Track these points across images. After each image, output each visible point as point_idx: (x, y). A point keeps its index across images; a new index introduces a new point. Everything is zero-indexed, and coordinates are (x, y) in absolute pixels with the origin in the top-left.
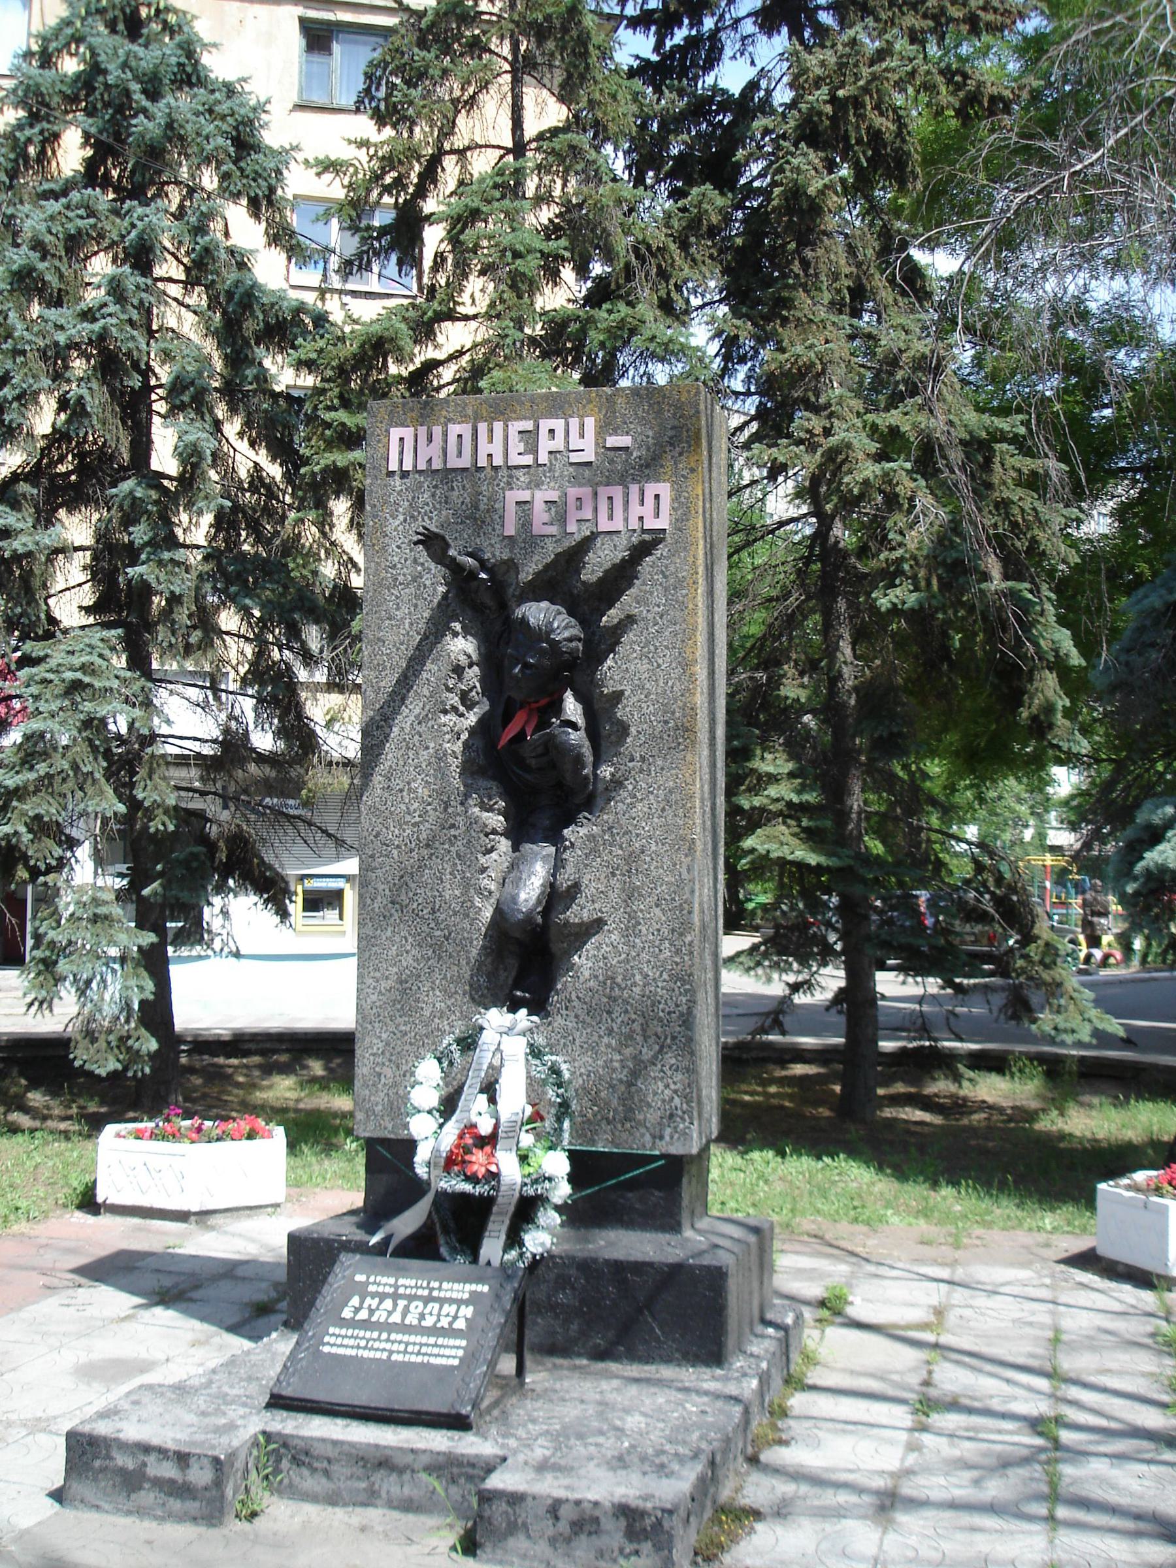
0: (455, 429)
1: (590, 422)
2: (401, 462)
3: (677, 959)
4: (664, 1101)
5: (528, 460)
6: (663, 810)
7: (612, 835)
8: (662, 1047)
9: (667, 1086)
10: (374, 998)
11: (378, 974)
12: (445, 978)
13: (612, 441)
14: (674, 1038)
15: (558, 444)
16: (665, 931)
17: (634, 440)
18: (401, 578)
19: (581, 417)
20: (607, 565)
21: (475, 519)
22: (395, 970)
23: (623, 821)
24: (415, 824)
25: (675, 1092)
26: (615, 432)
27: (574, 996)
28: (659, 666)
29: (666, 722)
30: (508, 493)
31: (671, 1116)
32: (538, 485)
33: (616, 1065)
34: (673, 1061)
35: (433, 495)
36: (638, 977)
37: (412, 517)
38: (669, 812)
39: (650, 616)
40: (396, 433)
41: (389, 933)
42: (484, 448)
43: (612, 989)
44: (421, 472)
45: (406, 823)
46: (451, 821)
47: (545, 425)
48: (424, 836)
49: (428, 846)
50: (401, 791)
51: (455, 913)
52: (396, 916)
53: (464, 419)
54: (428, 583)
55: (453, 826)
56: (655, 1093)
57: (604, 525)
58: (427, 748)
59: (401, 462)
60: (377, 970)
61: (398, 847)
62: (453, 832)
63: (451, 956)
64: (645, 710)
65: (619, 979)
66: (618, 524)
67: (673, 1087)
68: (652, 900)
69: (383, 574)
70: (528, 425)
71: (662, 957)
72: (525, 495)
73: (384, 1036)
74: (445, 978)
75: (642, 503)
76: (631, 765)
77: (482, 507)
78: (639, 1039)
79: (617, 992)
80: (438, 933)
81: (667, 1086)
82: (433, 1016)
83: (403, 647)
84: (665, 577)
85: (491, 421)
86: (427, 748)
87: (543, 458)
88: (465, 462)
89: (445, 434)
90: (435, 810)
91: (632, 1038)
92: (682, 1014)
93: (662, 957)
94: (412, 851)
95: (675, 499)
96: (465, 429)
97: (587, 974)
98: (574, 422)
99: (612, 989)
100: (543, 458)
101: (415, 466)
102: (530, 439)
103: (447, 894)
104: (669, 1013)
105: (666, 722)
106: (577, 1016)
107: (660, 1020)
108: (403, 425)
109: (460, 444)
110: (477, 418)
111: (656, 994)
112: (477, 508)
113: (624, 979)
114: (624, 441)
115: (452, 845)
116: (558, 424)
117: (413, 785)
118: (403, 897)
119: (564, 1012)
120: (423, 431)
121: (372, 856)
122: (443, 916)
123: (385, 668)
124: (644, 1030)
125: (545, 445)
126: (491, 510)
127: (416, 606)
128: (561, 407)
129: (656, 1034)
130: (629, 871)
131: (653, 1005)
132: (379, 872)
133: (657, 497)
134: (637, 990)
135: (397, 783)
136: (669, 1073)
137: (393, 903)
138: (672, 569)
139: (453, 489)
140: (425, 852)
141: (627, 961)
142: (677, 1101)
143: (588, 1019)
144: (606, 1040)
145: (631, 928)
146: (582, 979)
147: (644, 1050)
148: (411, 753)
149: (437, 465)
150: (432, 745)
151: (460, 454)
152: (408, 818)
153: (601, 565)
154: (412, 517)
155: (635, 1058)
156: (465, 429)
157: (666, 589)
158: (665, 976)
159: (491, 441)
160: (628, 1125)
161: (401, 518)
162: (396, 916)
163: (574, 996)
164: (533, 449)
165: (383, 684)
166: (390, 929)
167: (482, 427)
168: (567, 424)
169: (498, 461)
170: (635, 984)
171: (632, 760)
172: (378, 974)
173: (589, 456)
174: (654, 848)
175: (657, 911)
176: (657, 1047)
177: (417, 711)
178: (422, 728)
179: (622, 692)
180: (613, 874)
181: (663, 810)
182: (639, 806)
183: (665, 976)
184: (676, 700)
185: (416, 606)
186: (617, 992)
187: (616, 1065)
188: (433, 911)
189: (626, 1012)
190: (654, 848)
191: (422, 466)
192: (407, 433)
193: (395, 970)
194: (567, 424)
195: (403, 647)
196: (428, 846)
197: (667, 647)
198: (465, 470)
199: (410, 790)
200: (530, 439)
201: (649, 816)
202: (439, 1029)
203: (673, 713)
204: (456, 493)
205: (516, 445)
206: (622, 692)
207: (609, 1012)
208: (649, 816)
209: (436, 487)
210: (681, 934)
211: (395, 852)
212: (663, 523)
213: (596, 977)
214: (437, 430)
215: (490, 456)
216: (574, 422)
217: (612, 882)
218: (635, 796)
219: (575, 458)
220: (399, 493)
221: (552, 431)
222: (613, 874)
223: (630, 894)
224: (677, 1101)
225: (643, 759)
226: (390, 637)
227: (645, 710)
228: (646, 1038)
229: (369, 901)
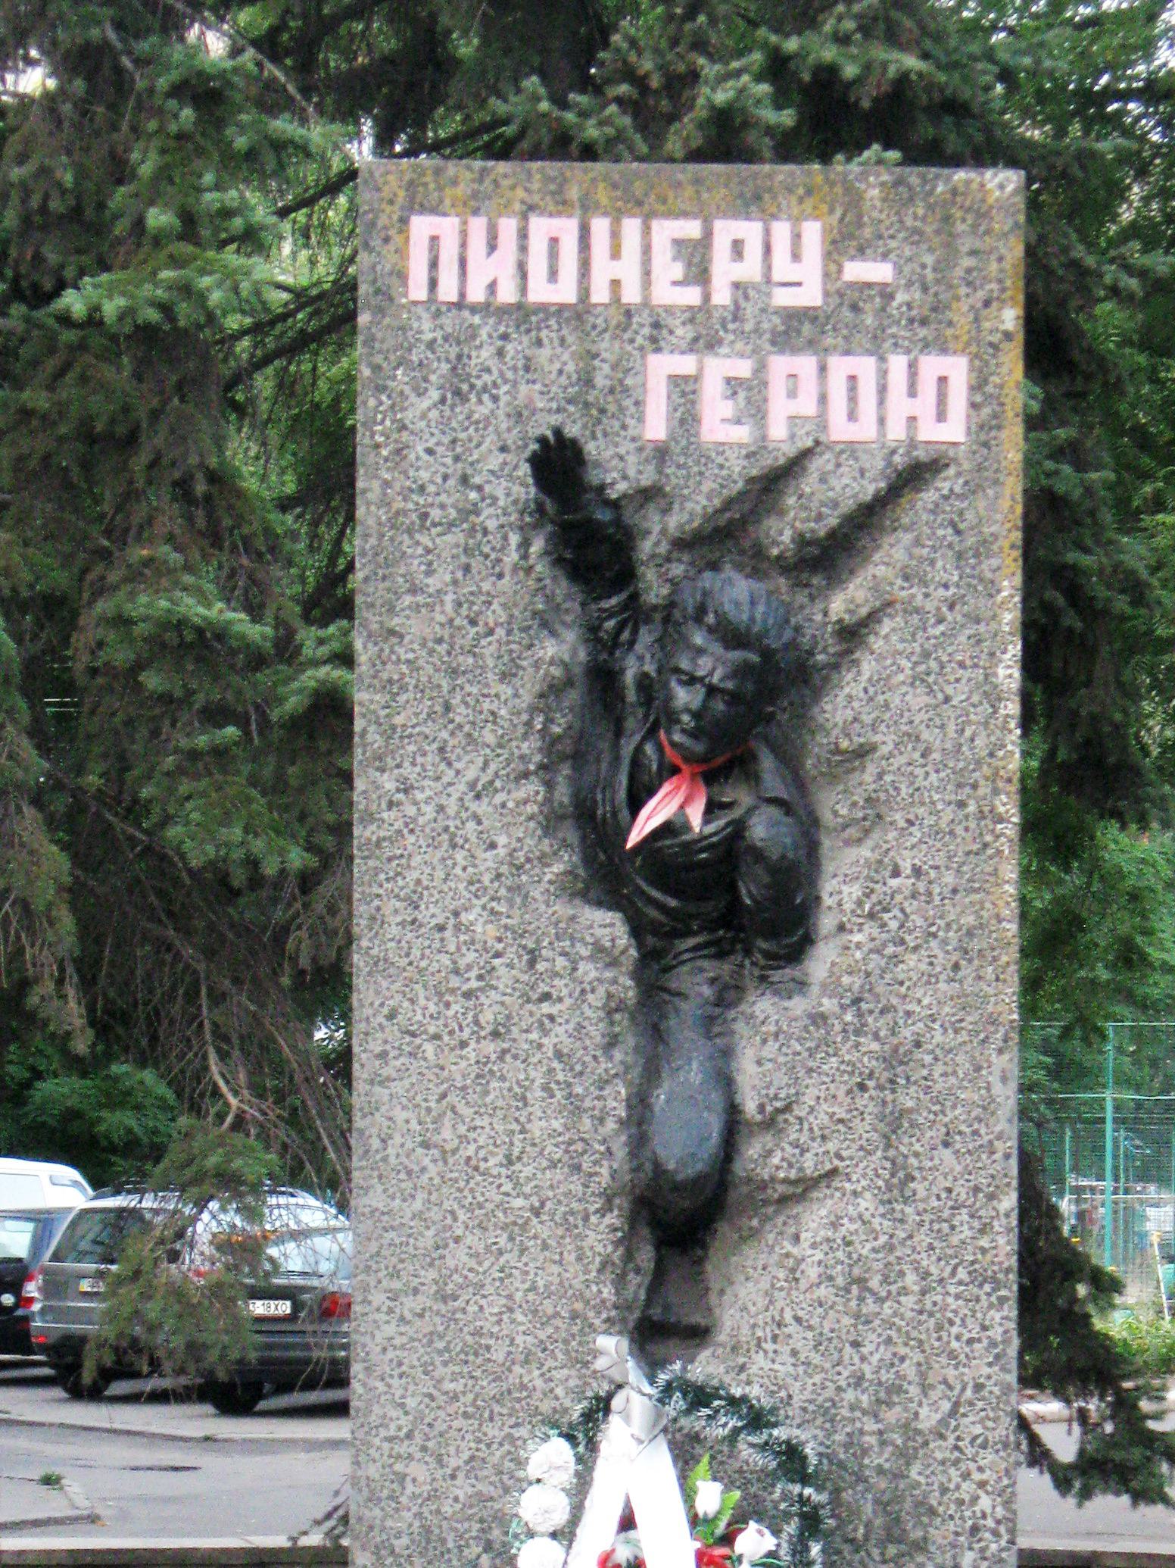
0: (541, 227)
1: (813, 232)
2: (433, 284)
3: (984, 1242)
4: (960, 1502)
5: (691, 296)
6: (956, 967)
7: (860, 1015)
8: (957, 1405)
9: (966, 1476)
10: (390, 1330)
11: (397, 1285)
12: (533, 1288)
13: (856, 271)
14: (979, 1387)
15: (750, 269)
16: (962, 1192)
17: (899, 270)
18: (435, 514)
19: (796, 221)
20: (848, 505)
21: (587, 405)
22: (432, 1274)
23: (880, 989)
24: (468, 995)
25: (982, 1485)
26: (861, 252)
27: (788, 1316)
28: (947, 699)
29: (962, 804)
30: (653, 359)
31: (975, 1530)
32: (712, 345)
33: (872, 1440)
34: (978, 1430)
35: (500, 353)
36: (911, 1278)
37: (457, 393)
38: (967, 971)
39: (929, 606)
40: (422, 226)
41: (418, 1205)
42: (602, 270)
43: (861, 1299)
44: (474, 309)
45: (453, 991)
46: (543, 988)
47: (726, 230)
48: (487, 1017)
49: (496, 1034)
50: (441, 928)
51: (553, 1165)
52: (433, 1170)
53: (562, 206)
54: (492, 525)
55: (546, 997)
56: (944, 1490)
57: (840, 429)
58: (493, 846)
59: (433, 284)
60: (395, 1274)
61: (437, 1037)
62: (546, 1008)
63: (545, 1246)
64: (920, 782)
65: (874, 1283)
66: (865, 430)
67: (977, 1476)
68: (936, 1134)
69: (399, 504)
70: (692, 229)
71: (955, 1240)
72: (686, 364)
73: (411, 1403)
74: (533, 1288)
75: (912, 392)
76: (894, 883)
77: (600, 381)
78: (914, 1391)
79: (870, 1306)
80: (519, 1202)
81: (966, 1476)
82: (510, 1361)
83: (442, 649)
84: (958, 532)
85: (617, 218)
86: (493, 846)
87: (722, 296)
88: (566, 292)
89: (523, 235)
90: (510, 966)
91: (900, 1390)
92: (993, 1344)
93: (955, 1240)
94: (463, 1044)
95: (978, 385)
96: (567, 228)
97: (813, 1273)
98: (781, 231)
99: (861, 1299)
100: (722, 296)
101: (462, 295)
102: (697, 263)
103: (536, 1128)
104: (970, 1341)
105: (962, 804)
106: (794, 1353)
107: (952, 1355)
108: (435, 210)
109: (553, 254)
110: (587, 207)
111: (945, 1308)
112: (588, 382)
113: (886, 1280)
114: (880, 272)
115: (546, 1033)
116: (750, 231)
117: (464, 917)
118: (447, 1133)
119: (769, 1346)
120: (478, 226)
121: (383, 1055)
122: (528, 1171)
123: (404, 688)
124: (923, 1376)
125: (724, 272)
126: (618, 389)
127: (467, 569)
128: (757, 198)
129: (945, 1382)
130: (892, 1082)
131: (939, 1328)
132: (398, 1087)
133: (943, 380)
134: (908, 1301)
135: (431, 913)
136: (970, 1451)
137: (425, 1145)
138: (969, 516)
139: (539, 343)
140: (490, 1048)
141: (890, 1248)
142: (985, 1502)
143: (816, 1359)
144: (850, 1395)
145: (899, 1184)
146: (803, 1284)
147: (924, 1412)
148: (460, 856)
149: (507, 294)
150: (502, 840)
151: (553, 275)
152: (455, 982)
153: (836, 505)
154: (457, 393)
155: (906, 1426)
156: (567, 228)
157: (960, 556)
158: (962, 1274)
159: (616, 254)
160: (892, 1550)
161: (435, 395)
162: (433, 1170)
163: (788, 1316)
164: (699, 273)
165: (398, 720)
166: (421, 1196)
167: (600, 226)
168: (767, 232)
169: (631, 295)
170: (904, 1291)
171: (896, 873)
172: (397, 1285)
173: (811, 295)
174: (938, 1038)
175: (947, 1154)
176: (946, 1406)
177: (471, 774)
178: (482, 808)
179: (873, 748)
180: (862, 1087)
181: (956, 967)
182: (911, 960)
183: (962, 1274)
184: (978, 763)
185: (467, 569)
186: (870, 1306)
187: (872, 1440)
188: (510, 1161)
189: (889, 1341)
190: (938, 1038)
191: (476, 294)
192: (447, 226)
193: (432, 1274)
194: (767, 232)
195: (442, 649)
196: (496, 1034)
197: (962, 665)
198: (562, 308)
199: (457, 928)
200: (697, 263)
201: (931, 979)
202: (523, 1387)
203: (975, 786)
204: (545, 353)
205: (668, 269)
206: (873, 748)
207: (856, 1344)
208: (931, 979)
209: (505, 337)
210: (991, 1197)
211: (429, 1048)
212: (954, 430)
213: (831, 1278)
214: (508, 226)
215: (616, 284)
216: (781, 231)
217: (860, 1103)
218: (902, 942)
219: (783, 298)
220: (431, 345)
221: (738, 248)
222: (862, 1087)
223: (894, 1123)
224: (985, 1502)
225: (917, 872)
226: (415, 627)
227: (920, 782)
228: (925, 1388)
229: (376, 1143)
